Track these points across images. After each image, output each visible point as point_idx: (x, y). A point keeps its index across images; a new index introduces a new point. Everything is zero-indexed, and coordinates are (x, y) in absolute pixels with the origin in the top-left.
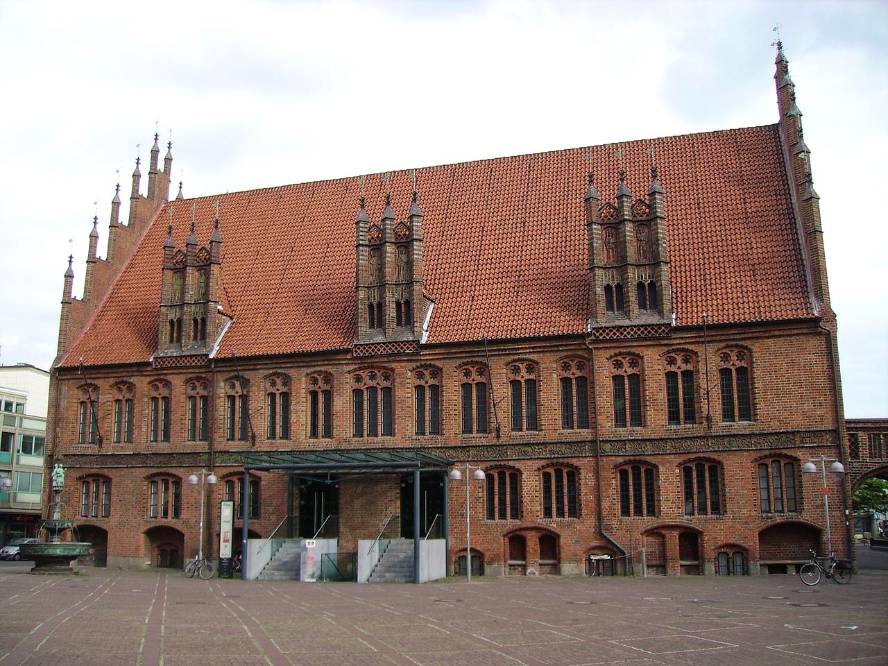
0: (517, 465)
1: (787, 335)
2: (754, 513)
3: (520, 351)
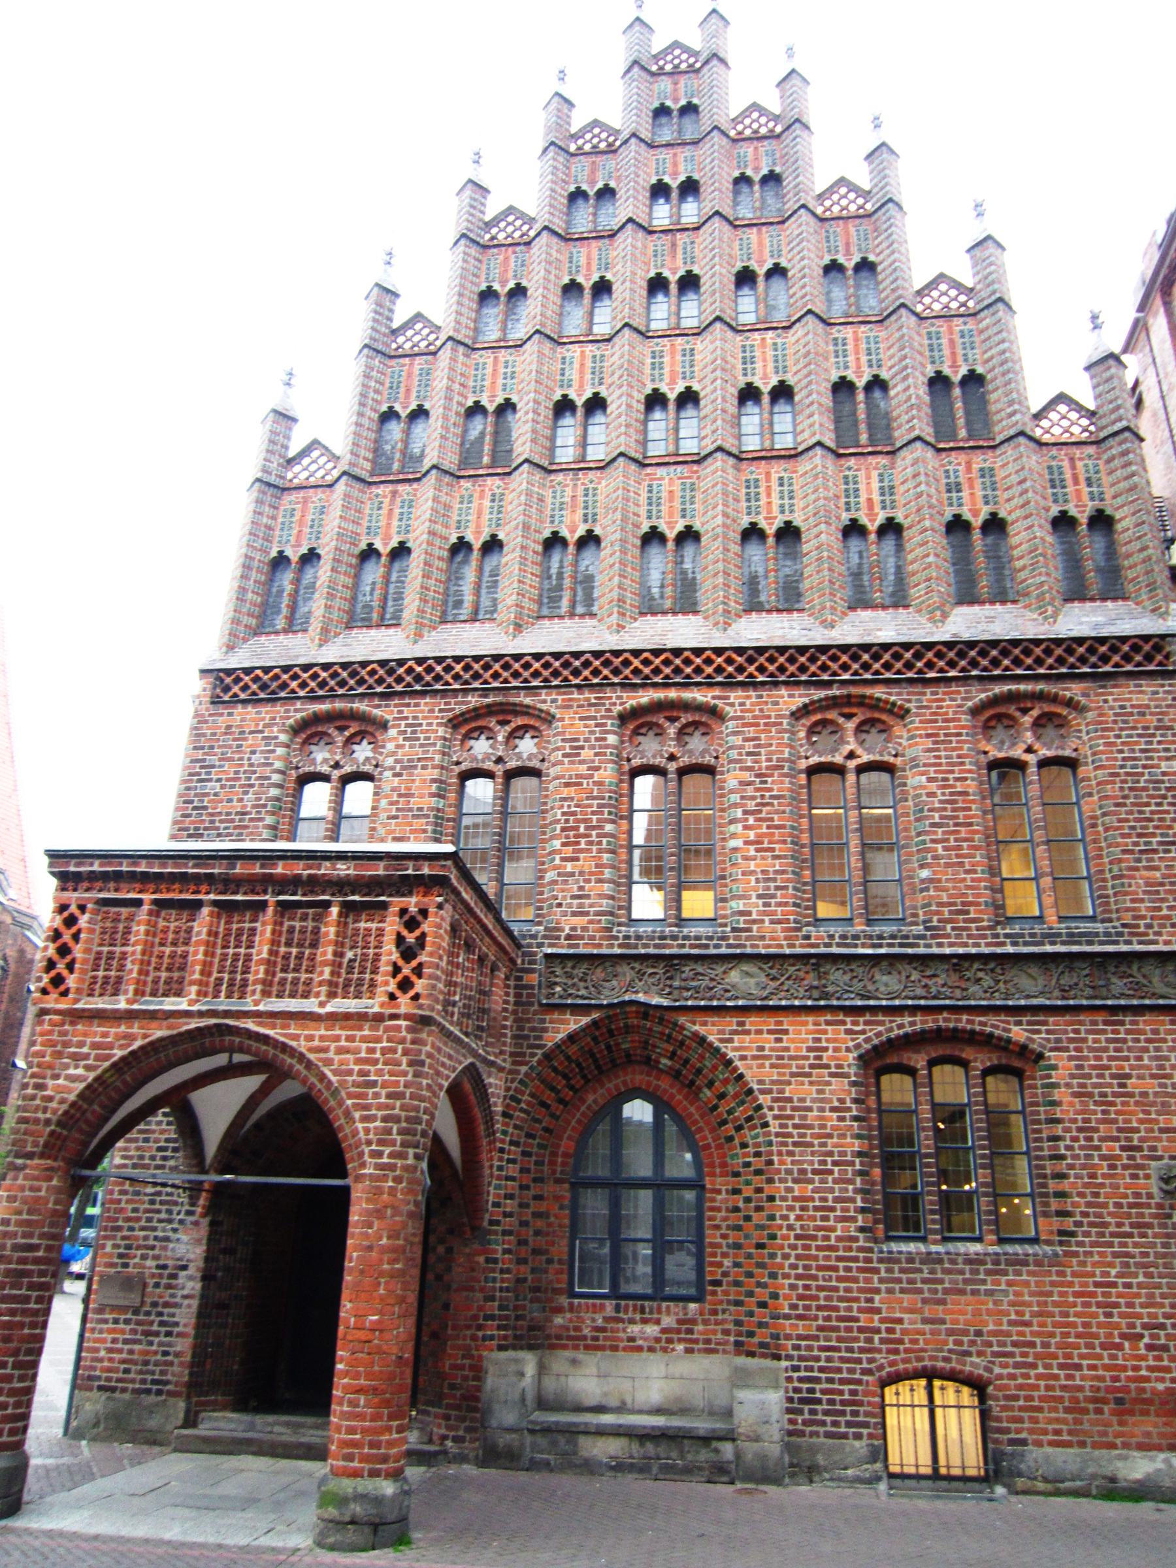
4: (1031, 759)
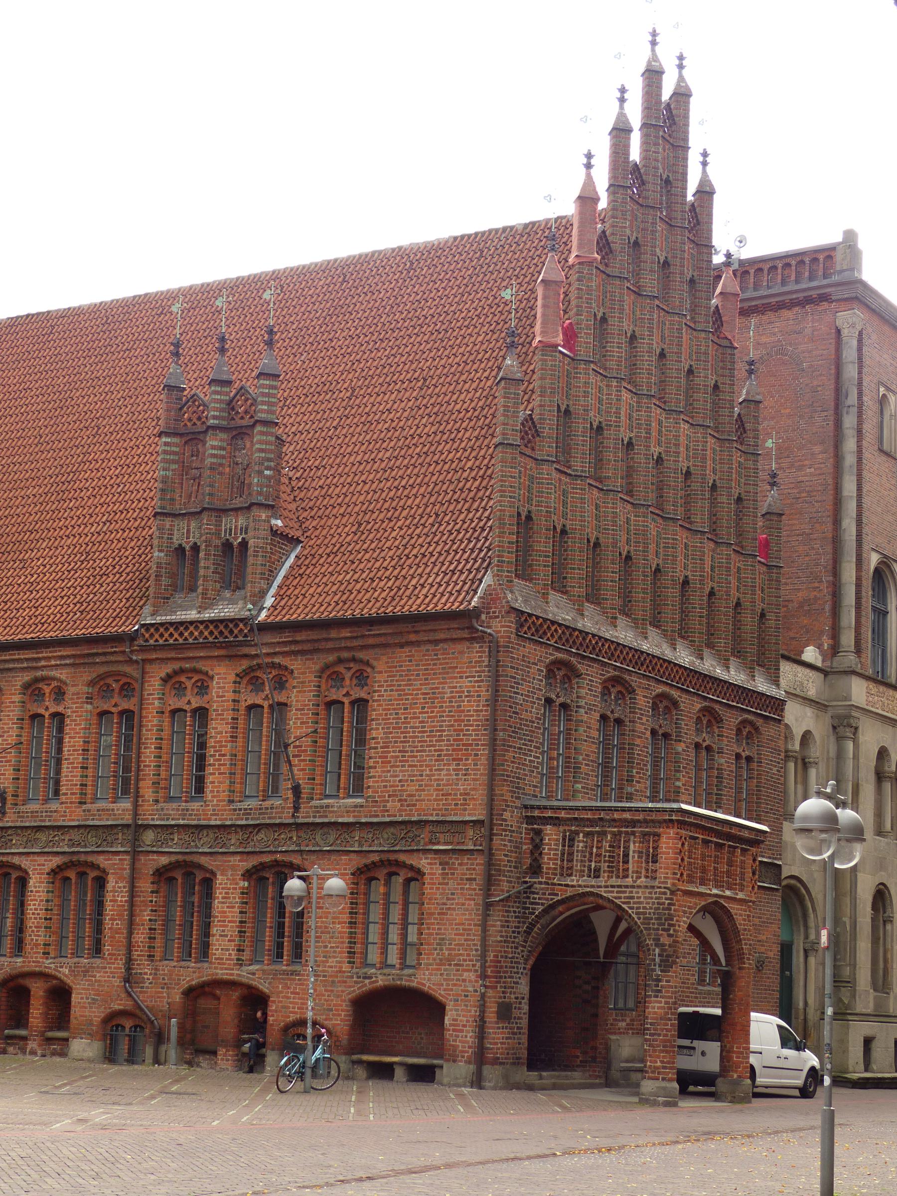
0: (25, 863)
1: (430, 642)
2: (346, 967)
3: (43, 663)
4: (743, 754)
